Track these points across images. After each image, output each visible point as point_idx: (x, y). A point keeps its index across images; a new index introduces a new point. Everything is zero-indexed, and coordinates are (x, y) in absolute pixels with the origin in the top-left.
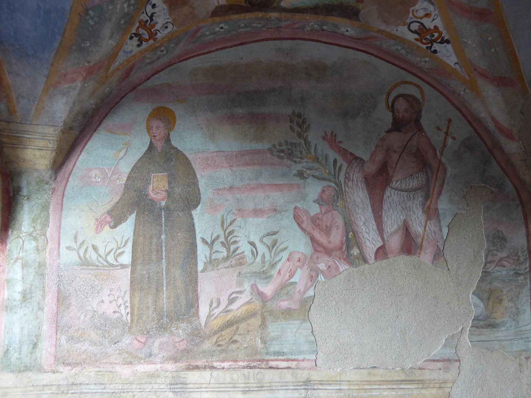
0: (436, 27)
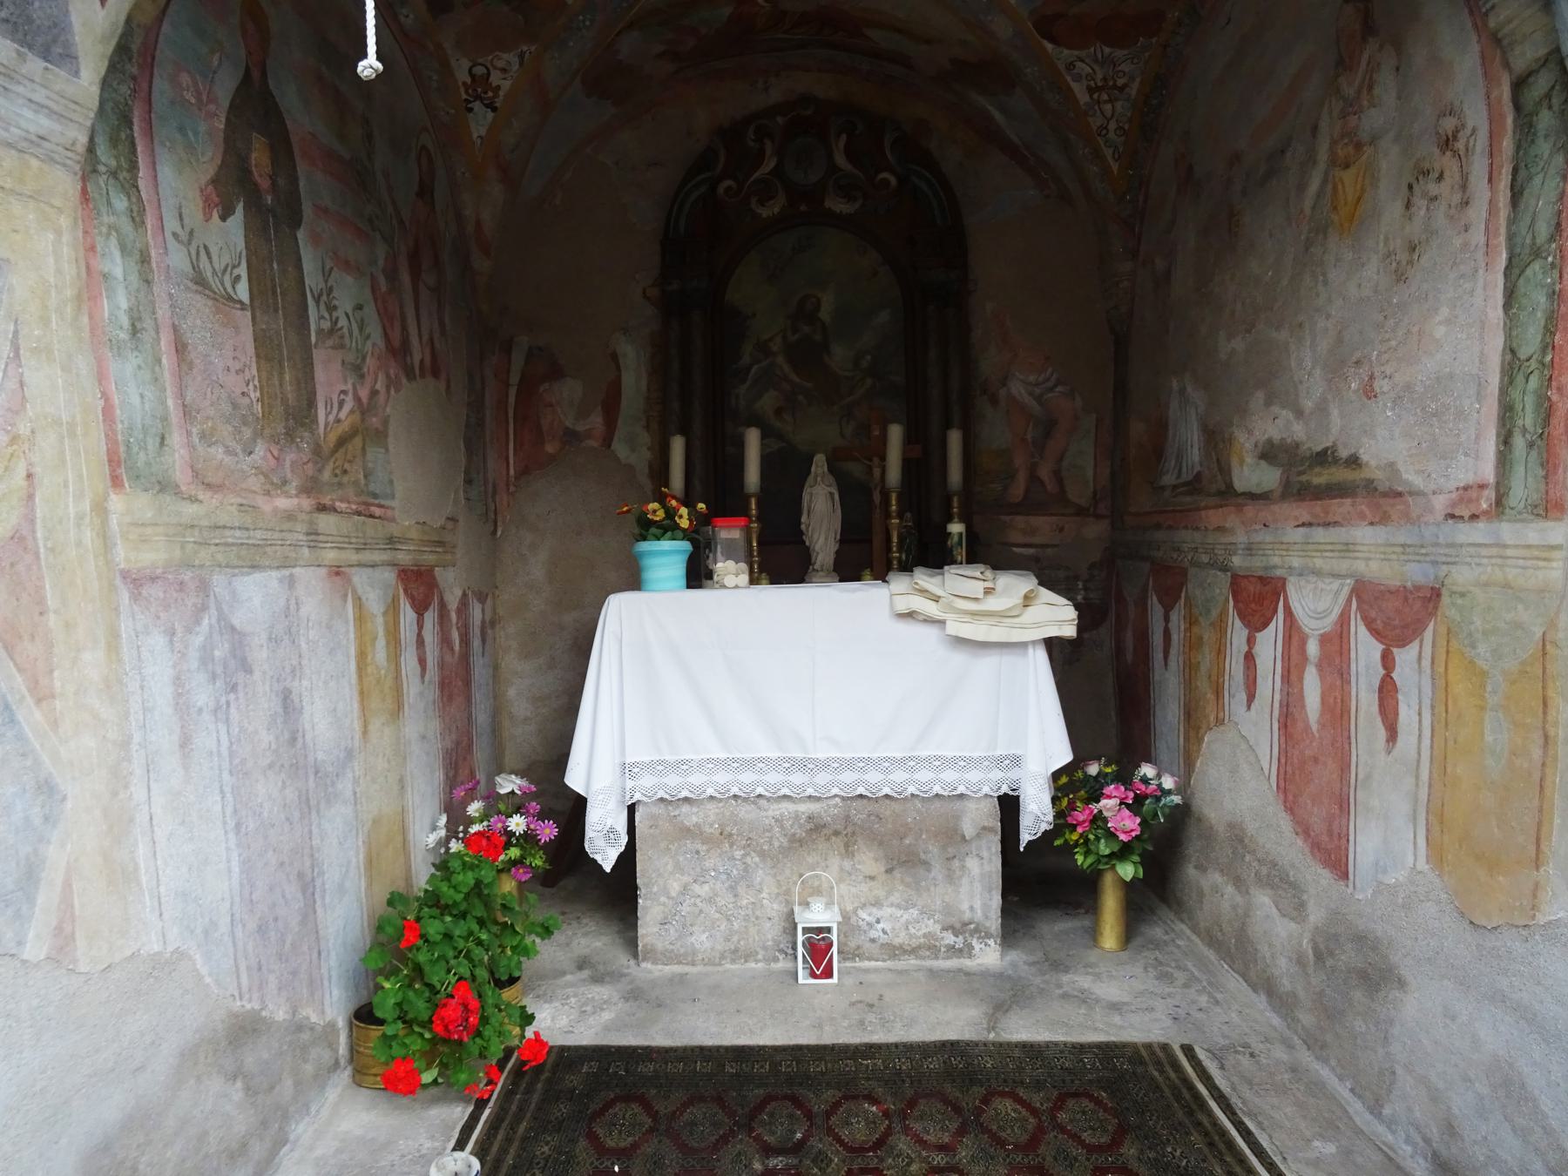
0: (498, 87)
